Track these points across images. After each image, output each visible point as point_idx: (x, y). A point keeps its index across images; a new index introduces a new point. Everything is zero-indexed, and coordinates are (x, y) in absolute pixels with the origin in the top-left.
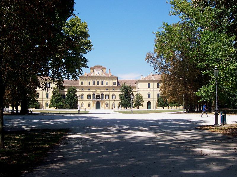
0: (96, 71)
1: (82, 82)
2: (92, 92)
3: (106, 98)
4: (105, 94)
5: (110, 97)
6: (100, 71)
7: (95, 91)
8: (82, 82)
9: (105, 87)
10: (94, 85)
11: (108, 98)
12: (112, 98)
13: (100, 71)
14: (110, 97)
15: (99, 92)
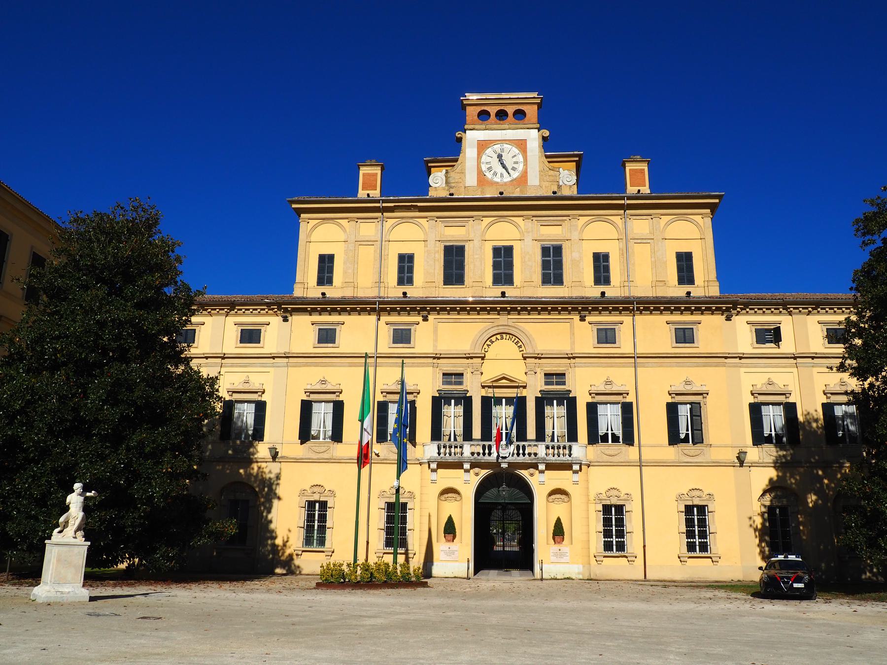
0: (482, 146)
1: (326, 263)
2: (430, 370)
3: (594, 437)
4: (582, 384)
5: (652, 425)
6: (521, 145)
7: (465, 347)
8: (326, 263)
9: (581, 307)
10: (453, 293)
11: (629, 439)
12: (674, 438)
13: (521, 145)
14: (652, 425)
15: (504, 362)
